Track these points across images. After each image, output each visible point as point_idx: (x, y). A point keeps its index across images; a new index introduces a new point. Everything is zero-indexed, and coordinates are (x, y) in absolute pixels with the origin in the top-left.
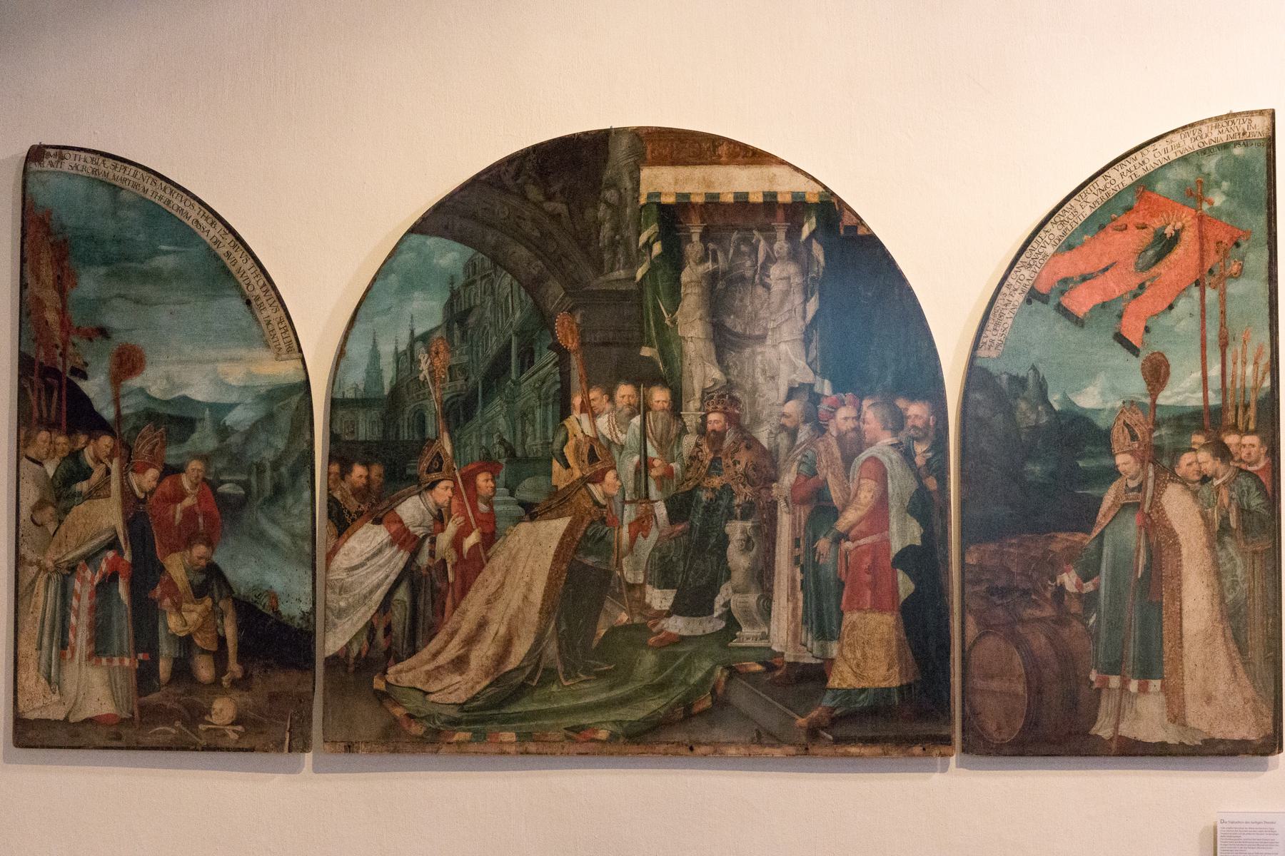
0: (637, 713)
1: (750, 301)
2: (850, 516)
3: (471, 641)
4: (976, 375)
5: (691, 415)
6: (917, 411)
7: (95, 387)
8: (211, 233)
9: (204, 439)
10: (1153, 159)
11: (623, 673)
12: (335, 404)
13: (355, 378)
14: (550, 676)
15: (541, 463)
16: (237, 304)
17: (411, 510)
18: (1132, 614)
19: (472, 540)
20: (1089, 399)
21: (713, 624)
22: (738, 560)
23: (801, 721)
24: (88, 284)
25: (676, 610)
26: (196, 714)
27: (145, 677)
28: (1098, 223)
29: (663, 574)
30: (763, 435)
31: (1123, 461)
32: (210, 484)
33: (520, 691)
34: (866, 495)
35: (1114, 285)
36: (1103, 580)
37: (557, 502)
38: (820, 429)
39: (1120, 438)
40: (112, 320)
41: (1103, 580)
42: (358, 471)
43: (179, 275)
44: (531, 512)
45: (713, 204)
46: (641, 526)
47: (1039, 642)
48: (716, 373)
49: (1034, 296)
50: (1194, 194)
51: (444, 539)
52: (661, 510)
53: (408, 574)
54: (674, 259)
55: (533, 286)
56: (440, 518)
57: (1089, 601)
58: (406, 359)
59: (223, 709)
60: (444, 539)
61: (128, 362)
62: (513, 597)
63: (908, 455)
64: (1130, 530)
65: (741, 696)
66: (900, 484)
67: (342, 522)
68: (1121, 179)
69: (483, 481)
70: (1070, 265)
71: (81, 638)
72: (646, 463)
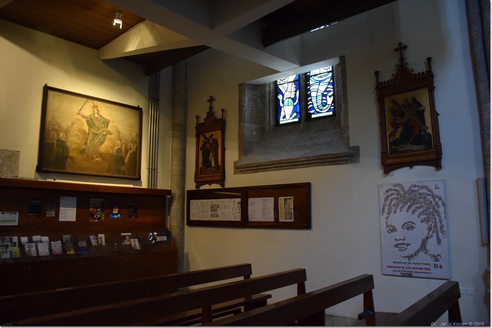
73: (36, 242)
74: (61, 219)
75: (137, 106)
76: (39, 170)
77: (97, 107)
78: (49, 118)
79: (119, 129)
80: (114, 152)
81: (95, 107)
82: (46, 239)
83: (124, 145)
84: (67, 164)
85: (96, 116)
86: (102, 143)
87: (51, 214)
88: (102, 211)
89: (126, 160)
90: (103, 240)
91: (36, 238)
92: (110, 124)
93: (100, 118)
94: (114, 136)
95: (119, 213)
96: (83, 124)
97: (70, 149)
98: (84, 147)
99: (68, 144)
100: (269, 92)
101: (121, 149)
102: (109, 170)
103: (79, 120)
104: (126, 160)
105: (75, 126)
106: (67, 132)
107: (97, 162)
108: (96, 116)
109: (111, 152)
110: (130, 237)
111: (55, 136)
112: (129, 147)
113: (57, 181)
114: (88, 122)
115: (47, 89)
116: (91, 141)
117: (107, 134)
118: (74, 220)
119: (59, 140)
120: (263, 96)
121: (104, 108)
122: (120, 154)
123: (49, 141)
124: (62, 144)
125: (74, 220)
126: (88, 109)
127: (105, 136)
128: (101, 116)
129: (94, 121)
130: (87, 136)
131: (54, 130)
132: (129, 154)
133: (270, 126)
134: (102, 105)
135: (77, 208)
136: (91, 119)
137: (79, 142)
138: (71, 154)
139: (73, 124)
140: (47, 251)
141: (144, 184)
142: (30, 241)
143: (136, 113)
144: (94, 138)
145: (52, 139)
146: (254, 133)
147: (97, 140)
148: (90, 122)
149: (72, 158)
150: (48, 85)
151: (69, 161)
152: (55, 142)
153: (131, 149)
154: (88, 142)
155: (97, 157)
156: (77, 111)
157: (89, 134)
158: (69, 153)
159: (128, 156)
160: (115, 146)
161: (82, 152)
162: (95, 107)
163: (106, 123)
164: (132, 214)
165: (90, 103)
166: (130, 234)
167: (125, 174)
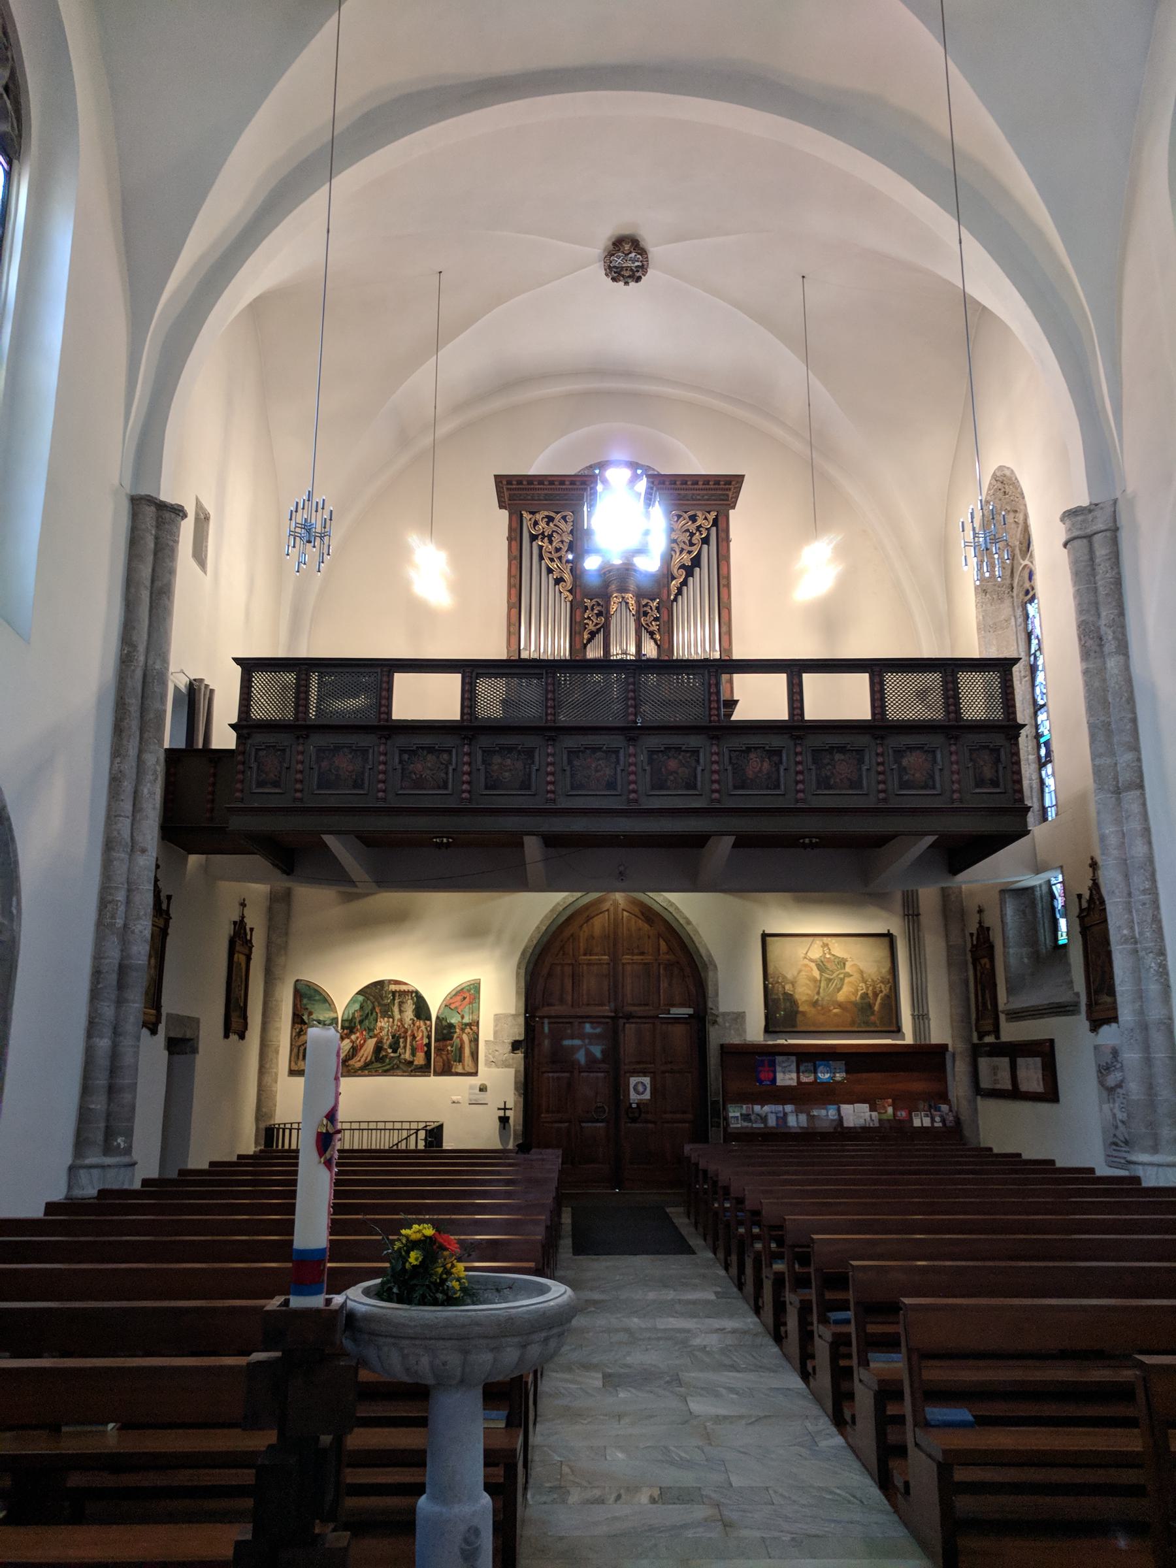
0: (385, 1068)
1: (404, 1005)
2: (418, 1039)
3: (361, 1057)
4: (438, 1018)
5: (396, 1022)
6: (428, 1022)
7: (305, 1018)
8: (324, 994)
10: (464, 985)
11: (384, 1062)
12: (342, 1021)
13: (346, 1017)
14: (373, 1063)
16: (327, 1005)
17: (353, 1037)
18: (458, 1055)
19: (362, 1042)
20: (453, 1021)
21: (397, 1055)
22: (402, 1045)
23: (410, 1069)
24: (305, 1001)
25: (393, 1052)
28: (455, 995)
29: (390, 1047)
30: (406, 1026)
31: (457, 1030)
33: (368, 1065)
34: (420, 1035)
35: (457, 1004)
36: (454, 1048)
37: (375, 1036)
38: (414, 1025)
39: (457, 1027)
40: (308, 1007)
41: (454, 1048)
42: (345, 1031)
43: (319, 1000)
44: (371, 1037)
45: (400, 991)
46: (387, 1040)
47: (445, 1057)
48: (399, 1017)
49: (446, 1006)
50: (469, 991)
51: (358, 1042)
52: (390, 1037)
54: (394, 999)
55: (373, 1003)
56: (357, 1038)
57: (452, 1051)
58: (354, 1014)
60: (358, 1042)
61: (310, 1014)
62: (368, 1050)
63: (426, 1029)
65: (401, 1066)
66: (426, 1034)
68: (459, 988)
69: (364, 1033)
70: (451, 1001)
72: (388, 1030)
75: (886, 932)
76: (767, 1030)
77: (827, 945)
78: (771, 970)
79: (861, 968)
81: (825, 945)
83: (871, 988)
84: (798, 1022)
85: (828, 956)
86: (839, 990)
89: (876, 1008)
92: (847, 963)
93: (833, 958)
94: (856, 976)
96: (812, 970)
97: (799, 1002)
98: (816, 997)
99: (797, 996)
100: (1041, 896)
101: (867, 994)
102: (853, 1023)
103: (806, 965)
104: (876, 1008)
105: (803, 973)
106: (793, 984)
107: (836, 1015)
108: (828, 956)
109: (853, 998)
111: (780, 989)
112: (878, 990)
114: (818, 966)
115: (765, 936)
116: (824, 990)
117: (844, 977)
119: (785, 994)
120: (1033, 904)
121: (836, 945)
122: (866, 1001)
124: (789, 998)
126: (816, 951)
127: (842, 980)
128: (834, 955)
129: (825, 963)
130: (818, 984)
132: (879, 998)
133: (1046, 948)
134: (834, 941)
136: (822, 962)
137: (810, 992)
138: (801, 1009)
139: (800, 971)
141: (909, 1039)
143: (886, 940)
144: (828, 985)
145: (777, 994)
146: (1026, 960)
147: (832, 987)
148: (821, 966)
149: (804, 1013)
151: (799, 1018)
153: (881, 991)
154: (821, 991)
155: (834, 1008)
156: (803, 955)
157: (820, 981)
158: (798, 1007)
161: (815, 1004)
162: (825, 945)
163: (842, 963)
165: (818, 942)
167: (876, 1026)
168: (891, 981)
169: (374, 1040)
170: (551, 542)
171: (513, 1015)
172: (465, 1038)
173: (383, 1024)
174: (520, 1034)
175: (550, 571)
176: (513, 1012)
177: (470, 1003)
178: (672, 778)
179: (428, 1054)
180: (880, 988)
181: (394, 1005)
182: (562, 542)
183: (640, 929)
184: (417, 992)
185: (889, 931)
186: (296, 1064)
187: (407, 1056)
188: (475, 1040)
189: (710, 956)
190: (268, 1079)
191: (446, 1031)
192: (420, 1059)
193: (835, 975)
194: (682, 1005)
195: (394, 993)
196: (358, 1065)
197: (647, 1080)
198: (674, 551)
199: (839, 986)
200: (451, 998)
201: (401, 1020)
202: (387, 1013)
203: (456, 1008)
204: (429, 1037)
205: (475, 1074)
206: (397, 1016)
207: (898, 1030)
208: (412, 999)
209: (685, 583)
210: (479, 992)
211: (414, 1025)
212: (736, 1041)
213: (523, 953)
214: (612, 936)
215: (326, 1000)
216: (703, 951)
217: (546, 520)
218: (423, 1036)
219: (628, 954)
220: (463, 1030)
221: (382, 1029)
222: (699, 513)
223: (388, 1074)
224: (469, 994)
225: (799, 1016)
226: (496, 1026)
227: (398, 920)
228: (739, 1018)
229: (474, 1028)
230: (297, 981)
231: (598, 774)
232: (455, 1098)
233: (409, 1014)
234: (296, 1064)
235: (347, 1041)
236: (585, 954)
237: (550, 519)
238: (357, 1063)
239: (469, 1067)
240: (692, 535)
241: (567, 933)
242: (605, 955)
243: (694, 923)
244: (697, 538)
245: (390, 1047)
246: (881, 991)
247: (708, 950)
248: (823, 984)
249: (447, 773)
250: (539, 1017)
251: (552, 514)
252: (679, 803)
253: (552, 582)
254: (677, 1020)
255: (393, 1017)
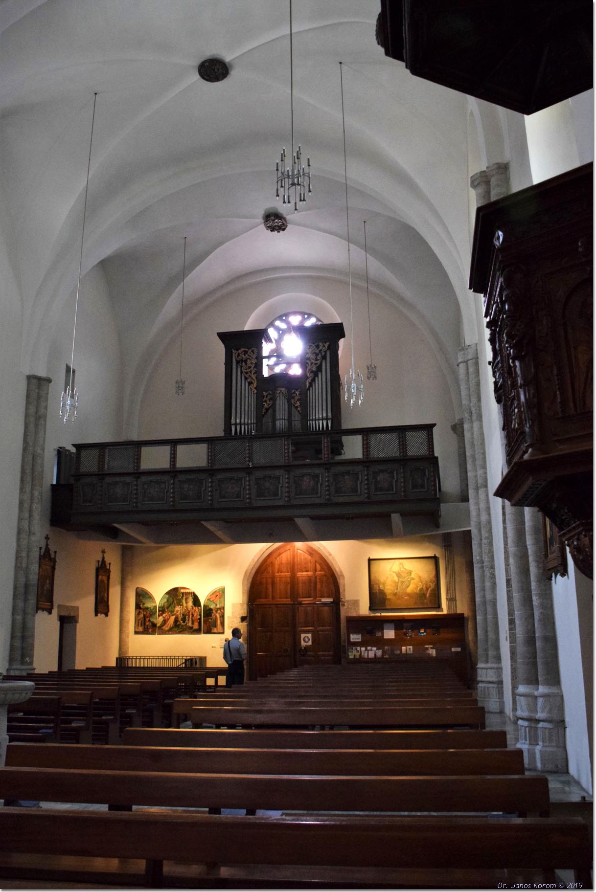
4: (204, 605)
6: (199, 608)
7: (141, 606)
9: (149, 610)
11: (179, 627)
12: (159, 607)
13: (160, 605)
15: (173, 612)
17: (164, 615)
21: (185, 624)
22: (187, 619)
24: (141, 598)
26: (148, 631)
27: (145, 628)
28: (212, 594)
30: (189, 610)
31: (214, 612)
32: (150, 613)
34: (196, 614)
35: (214, 598)
44: (173, 615)
45: (186, 593)
47: (208, 625)
49: (208, 599)
50: (219, 592)
53: (164, 620)
54: (183, 597)
55: (173, 598)
56: (166, 616)
58: (164, 604)
59: (150, 630)
61: (144, 604)
64: (214, 617)
66: (198, 614)
67: (159, 616)
68: (214, 591)
70: (211, 597)
71: (140, 625)
73: (368, 651)
74: (385, 637)
75: (433, 555)
76: (370, 609)
78: (372, 577)
80: (418, 590)
82: (374, 649)
83: (425, 585)
86: (408, 587)
87: (379, 634)
88: (412, 631)
89: (428, 595)
90: (412, 650)
91: (369, 648)
94: (417, 579)
95: (425, 632)
97: (387, 594)
98: (396, 591)
101: (423, 588)
102: (416, 603)
103: (391, 575)
104: (428, 595)
106: (384, 584)
107: (406, 600)
108: (402, 569)
109: (415, 591)
110: (431, 648)
112: (428, 586)
113: (383, 614)
114: (397, 574)
115: (370, 560)
117: (411, 580)
118: (394, 637)
119: (380, 590)
122: (423, 592)
123: (374, 591)
124: (382, 592)
125: (394, 637)
126: (395, 566)
127: (410, 581)
128: (405, 569)
129: (401, 573)
131: (377, 584)
135: (395, 630)
137: (392, 588)
138: (388, 597)
139: (387, 578)
140: (374, 655)
142: (366, 649)
144: (402, 584)
145: (376, 590)
148: (399, 575)
149: (389, 599)
150: (371, 558)
152: (377, 591)
154: (398, 588)
157: (398, 583)
158: (386, 596)
159: (429, 592)
160: (417, 587)
161: (395, 594)
162: (401, 564)
163: (410, 573)
164: (434, 632)
166: (432, 646)
168: (436, 581)
169: (174, 616)
170: (246, 364)
171: (241, 604)
172: (218, 615)
173: (178, 609)
174: (245, 614)
175: (246, 378)
176: (241, 602)
177: (220, 598)
178: (267, 491)
179: (200, 623)
180: (430, 585)
181: (183, 599)
182: (252, 363)
183: (306, 559)
184: (194, 593)
185: (435, 555)
186: (138, 628)
187: (190, 624)
188: (223, 616)
189: (341, 572)
190: (124, 636)
191: (208, 612)
192: (196, 626)
193: (406, 579)
194: (329, 597)
195: (183, 593)
196: (167, 629)
197: (310, 635)
198: (308, 364)
199: (408, 585)
200: (211, 596)
201: (187, 607)
202: (180, 603)
203: (213, 601)
204: (200, 615)
205: (223, 633)
206: (185, 605)
207: (439, 607)
208: (192, 596)
209: (313, 380)
210: (224, 593)
211: (193, 609)
212: (354, 614)
213: (246, 573)
214: (292, 563)
215: (149, 597)
216: (337, 569)
217: (243, 353)
218: (197, 615)
219: (299, 572)
220: (216, 611)
221: (177, 611)
222: (320, 344)
223: (182, 633)
224: (220, 594)
225: (387, 601)
226: (233, 609)
227: (184, 557)
228: (356, 603)
229: (222, 610)
230: (137, 588)
231: (233, 490)
232: (213, 645)
233: (190, 604)
234: (138, 628)
235: (161, 617)
236: (278, 573)
237: (246, 353)
238: (166, 628)
239: (220, 630)
240: (317, 355)
241: (269, 562)
242: (288, 572)
243: (333, 555)
244: (319, 357)
245: (182, 620)
246: (430, 587)
247: (340, 569)
248: (400, 584)
249: (164, 493)
250: (256, 605)
251: (246, 350)
252: (270, 503)
253: (247, 384)
254: (325, 604)
255: (183, 605)
